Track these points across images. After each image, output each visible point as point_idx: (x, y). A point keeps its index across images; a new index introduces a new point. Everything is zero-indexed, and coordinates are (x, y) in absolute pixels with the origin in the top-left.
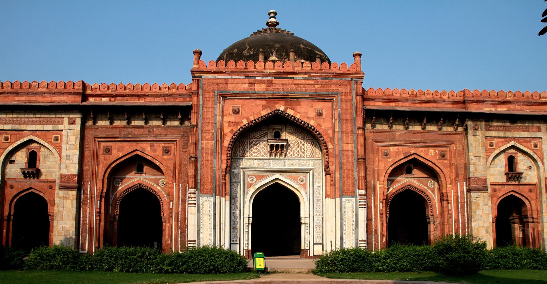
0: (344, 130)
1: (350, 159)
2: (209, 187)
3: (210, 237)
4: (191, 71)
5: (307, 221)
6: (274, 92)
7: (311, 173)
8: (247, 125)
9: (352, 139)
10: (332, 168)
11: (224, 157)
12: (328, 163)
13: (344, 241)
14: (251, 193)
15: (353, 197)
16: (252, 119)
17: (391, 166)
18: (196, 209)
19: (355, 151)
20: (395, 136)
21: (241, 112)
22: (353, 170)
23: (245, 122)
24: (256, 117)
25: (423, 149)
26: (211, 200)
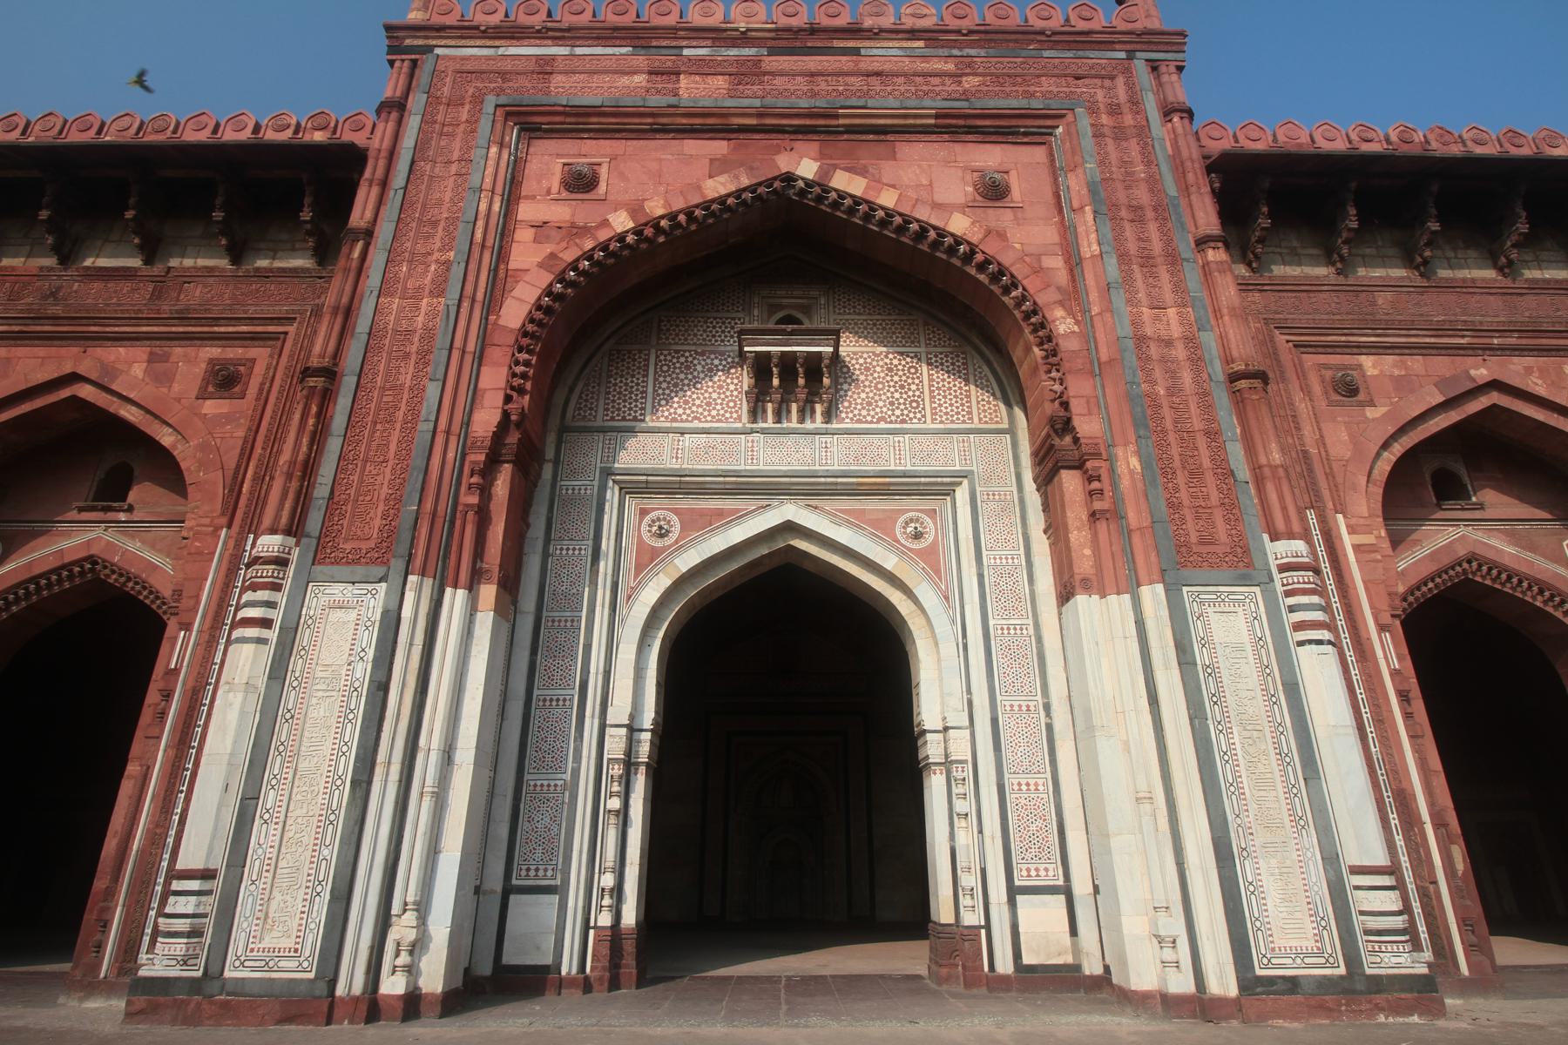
0: (1132, 247)
1: (1187, 378)
2: (378, 522)
3: (320, 843)
4: (389, 28)
5: (960, 749)
6: (769, 101)
7: (962, 494)
8: (630, 239)
9: (1179, 287)
10: (1087, 426)
11: (494, 378)
12: (1065, 405)
13: (1246, 871)
14: (651, 594)
15: (1245, 580)
16: (660, 212)
17: (1385, 446)
18: (267, 653)
19: (1209, 340)
20: (1374, 304)
21: (602, 188)
22: (1213, 434)
23: (622, 222)
24: (679, 204)
25: (1529, 361)
26: (375, 599)
